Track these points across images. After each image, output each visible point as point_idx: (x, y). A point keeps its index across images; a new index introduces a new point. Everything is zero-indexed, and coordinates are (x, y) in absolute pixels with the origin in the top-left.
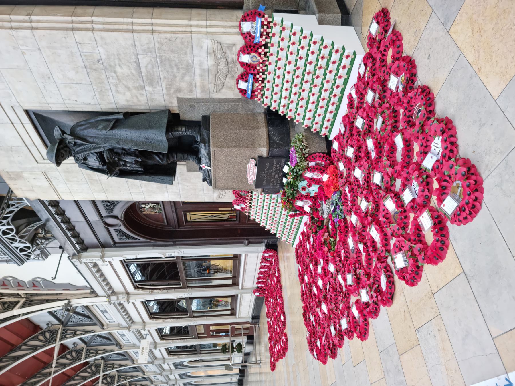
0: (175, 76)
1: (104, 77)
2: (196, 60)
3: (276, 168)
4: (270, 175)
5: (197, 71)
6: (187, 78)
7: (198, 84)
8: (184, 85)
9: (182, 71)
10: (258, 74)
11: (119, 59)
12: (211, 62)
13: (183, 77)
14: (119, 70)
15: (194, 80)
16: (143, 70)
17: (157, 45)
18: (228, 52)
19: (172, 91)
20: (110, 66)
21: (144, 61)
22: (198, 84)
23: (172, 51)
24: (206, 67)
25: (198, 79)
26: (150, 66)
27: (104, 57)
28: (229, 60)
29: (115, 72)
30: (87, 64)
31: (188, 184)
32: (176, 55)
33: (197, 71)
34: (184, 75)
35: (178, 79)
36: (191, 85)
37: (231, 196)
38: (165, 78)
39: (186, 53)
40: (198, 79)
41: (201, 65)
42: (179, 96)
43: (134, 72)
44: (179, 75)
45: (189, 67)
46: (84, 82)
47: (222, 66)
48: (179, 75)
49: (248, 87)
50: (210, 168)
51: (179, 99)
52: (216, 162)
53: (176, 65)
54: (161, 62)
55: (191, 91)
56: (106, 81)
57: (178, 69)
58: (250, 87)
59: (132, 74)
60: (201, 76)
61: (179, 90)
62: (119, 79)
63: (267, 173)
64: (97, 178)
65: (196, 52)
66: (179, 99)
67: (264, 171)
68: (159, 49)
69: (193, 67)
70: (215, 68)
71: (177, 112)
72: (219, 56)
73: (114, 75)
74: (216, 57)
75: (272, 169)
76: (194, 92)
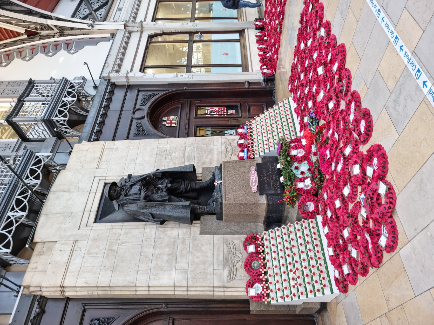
0: (203, 156)
1: (164, 158)
2: (215, 147)
3: (272, 171)
4: (269, 179)
5: (216, 152)
6: (210, 156)
7: (215, 159)
8: (207, 160)
9: (207, 153)
10: (260, 254)
11: (176, 149)
12: (223, 148)
13: (207, 156)
14: (173, 154)
15: (214, 157)
16: (186, 154)
17: (197, 142)
18: (232, 143)
19: (200, 163)
20: (170, 153)
21: (188, 149)
22: (215, 159)
23: (204, 144)
24: (220, 150)
25: (216, 157)
26: (190, 151)
27: (168, 149)
28: (233, 147)
29: (171, 156)
30: (158, 153)
31: (198, 254)
32: (205, 146)
33: (216, 152)
34: (208, 155)
35: (204, 157)
36: (211, 160)
37: (243, 275)
38: (197, 157)
39: (210, 145)
40: (216, 157)
41: (217, 149)
42: (203, 167)
43: (181, 155)
44: (205, 155)
45: (211, 151)
46: (152, 162)
47: (229, 149)
48: (205, 155)
49: (244, 155)
50: (221, 182)
51: (203, 169)
52: (226, 172)
53: (205, 150)
54: (197, 149)
55: (211, 163)
56: (164, 161)
57: (205, 152)
58: (246, 154)
59: (180, 156)
60: (217, 155)
61: (204, 163)
62: (171, 159)
63: (266, 176)
64: (116, 248)
65: (215, 144)
66: (203, 169)
67: (263, 175)
68: (197, 144)
69: (214, 151)
70: (225, 150)
71: (200, 178)
72: (227, 145)
73: (170, 157)
74: (226, 145)
75: (268, 172)
76: (213, 164)
